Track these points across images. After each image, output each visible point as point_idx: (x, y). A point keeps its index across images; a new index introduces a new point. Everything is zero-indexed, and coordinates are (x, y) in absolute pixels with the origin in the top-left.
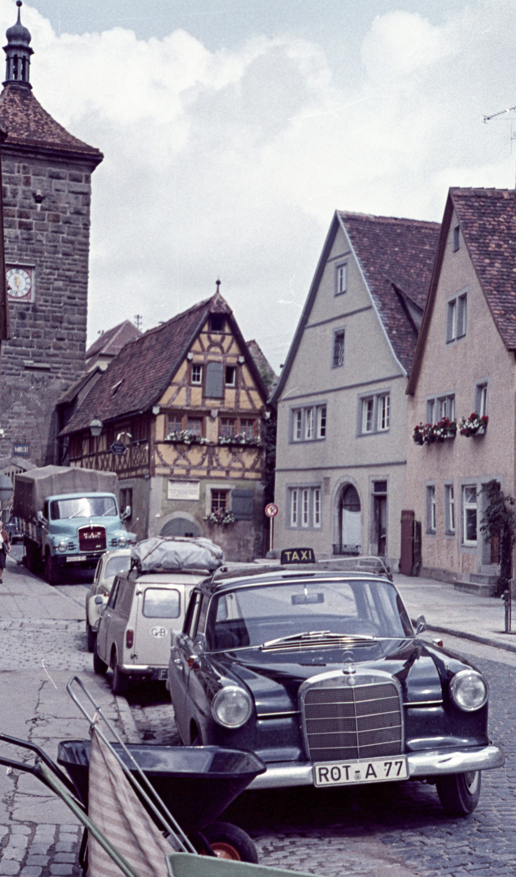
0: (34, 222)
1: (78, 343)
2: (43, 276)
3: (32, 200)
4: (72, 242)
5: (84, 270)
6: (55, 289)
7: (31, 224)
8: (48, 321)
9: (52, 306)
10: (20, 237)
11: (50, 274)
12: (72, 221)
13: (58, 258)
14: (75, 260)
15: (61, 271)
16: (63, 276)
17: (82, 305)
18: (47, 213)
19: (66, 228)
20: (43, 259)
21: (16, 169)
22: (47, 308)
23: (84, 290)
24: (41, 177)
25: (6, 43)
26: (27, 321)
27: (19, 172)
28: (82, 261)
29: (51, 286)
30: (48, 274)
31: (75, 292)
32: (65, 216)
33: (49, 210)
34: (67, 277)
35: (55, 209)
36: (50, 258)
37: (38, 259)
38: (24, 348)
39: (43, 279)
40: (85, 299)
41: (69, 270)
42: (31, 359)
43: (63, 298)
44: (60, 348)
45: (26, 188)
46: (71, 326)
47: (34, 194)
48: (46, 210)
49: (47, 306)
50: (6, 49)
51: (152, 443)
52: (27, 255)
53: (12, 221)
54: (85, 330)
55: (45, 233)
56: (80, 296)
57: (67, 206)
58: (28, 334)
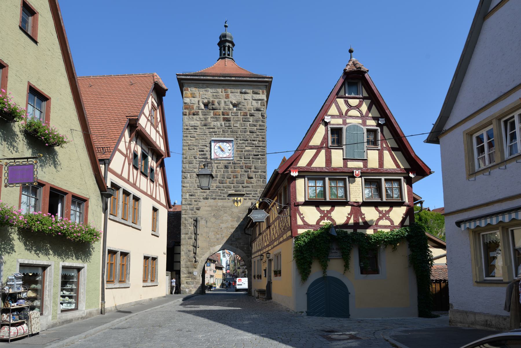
0: (232, 117)
1: (262, 180)
2: (238, 145)
3: (231, 107)
7: (230, 118)
9: (244, 161)
11: (243, 143)
13: (247, 135)
15: (249, 141)
18: (240, 111)
19: (251, 119)
20: (238, 136)
26: (230, 170)
29: (244, 150)
33: (241, 110)
35: (244, 109)
37: (235, 136)
38: (228, 184)
39: (239, 146)
42: (233, 190)
44: (251, 183)
45: (226, 100)
47: (231, 103)
48: (239, 110)
51: (292, 205)
52: (228, 135)
53: (219, 117)
54: (265, 172)
55: (239, 122)
58: (230, 176)
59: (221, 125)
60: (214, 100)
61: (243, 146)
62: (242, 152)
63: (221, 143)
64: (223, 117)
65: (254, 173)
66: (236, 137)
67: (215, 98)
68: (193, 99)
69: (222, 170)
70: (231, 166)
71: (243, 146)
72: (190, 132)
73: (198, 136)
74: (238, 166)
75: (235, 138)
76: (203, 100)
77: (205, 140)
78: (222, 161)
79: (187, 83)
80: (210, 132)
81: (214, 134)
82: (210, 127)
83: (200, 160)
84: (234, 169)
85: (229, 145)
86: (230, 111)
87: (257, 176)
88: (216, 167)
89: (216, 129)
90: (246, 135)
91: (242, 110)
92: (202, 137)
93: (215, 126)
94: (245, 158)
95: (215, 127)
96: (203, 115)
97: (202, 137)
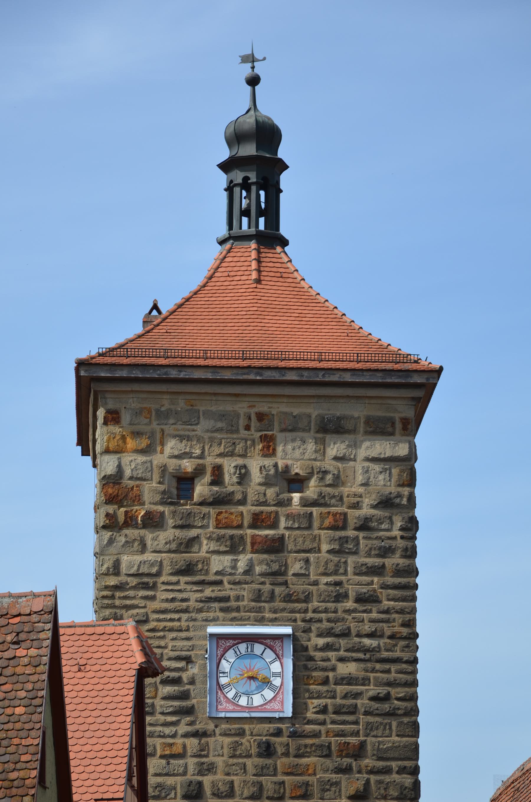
0: (287, 533)
4: (378, 571)
5: (405, 631)
6: (340, 681)
8: (328, 756)
9: (333, 722)
10: (258, 569)
11: (327, 647)
12: (374, 524)
14: (387, 611)
16: (358, 651)
17: (405, 714)
18: (315, 511)
20: (310, 615)
21: (242, 422)
22: (323, 728)
23: (409, 678)
24: (300, 434)
25: (224, 154)
27: (248, 428)
28: (401, 612)
29: (331, 675)
30: (322, 649)
31: (389, 684)
32: (357, 513)
34: (366, 650)
35: (333, 501)
36: (326, 611)
37: (298, 615)
40: (414, 698)
41: (371, 635)
43: (359, 702)
46: (381, 764)
48: (315, 504)
49: (324, 723)
50: (225, 167)
55: (312, 557)
56: (401, 692)
57: (361, 490)
59: (247, 572)
60: (219, 461)
61: (328, 660)
62: (326, 682)
63: (242, 647)
64: (253, 537)
65: (373, 778)
66: (304, 620)
67: (221, 455)
68: (141, 459)
69: (249, 762)
70: (281, 744)
71: (328, 660)
72: (128, 602)
73: (156, 616)
74: (306, 746)
75: (299, 623)
76: (174, 461)
77: (184, 634)
78: (246, 727)
79: (114, 392)
80: (201, 601)
81: (216, 605)
82: (202, 578)
83: (162, 718)
84: (296, 756)
85: (274, 656)
86: (279, 509)
87: (382, 791)
88: (226, 751)
89: (227, 585)
90: (340, 614)
91: (325, 505)
92: (171, 620)
93: (217, 573)
94: (334, 713)
95: (219, 578)
96: (175, 527)
97: (171, 620)
